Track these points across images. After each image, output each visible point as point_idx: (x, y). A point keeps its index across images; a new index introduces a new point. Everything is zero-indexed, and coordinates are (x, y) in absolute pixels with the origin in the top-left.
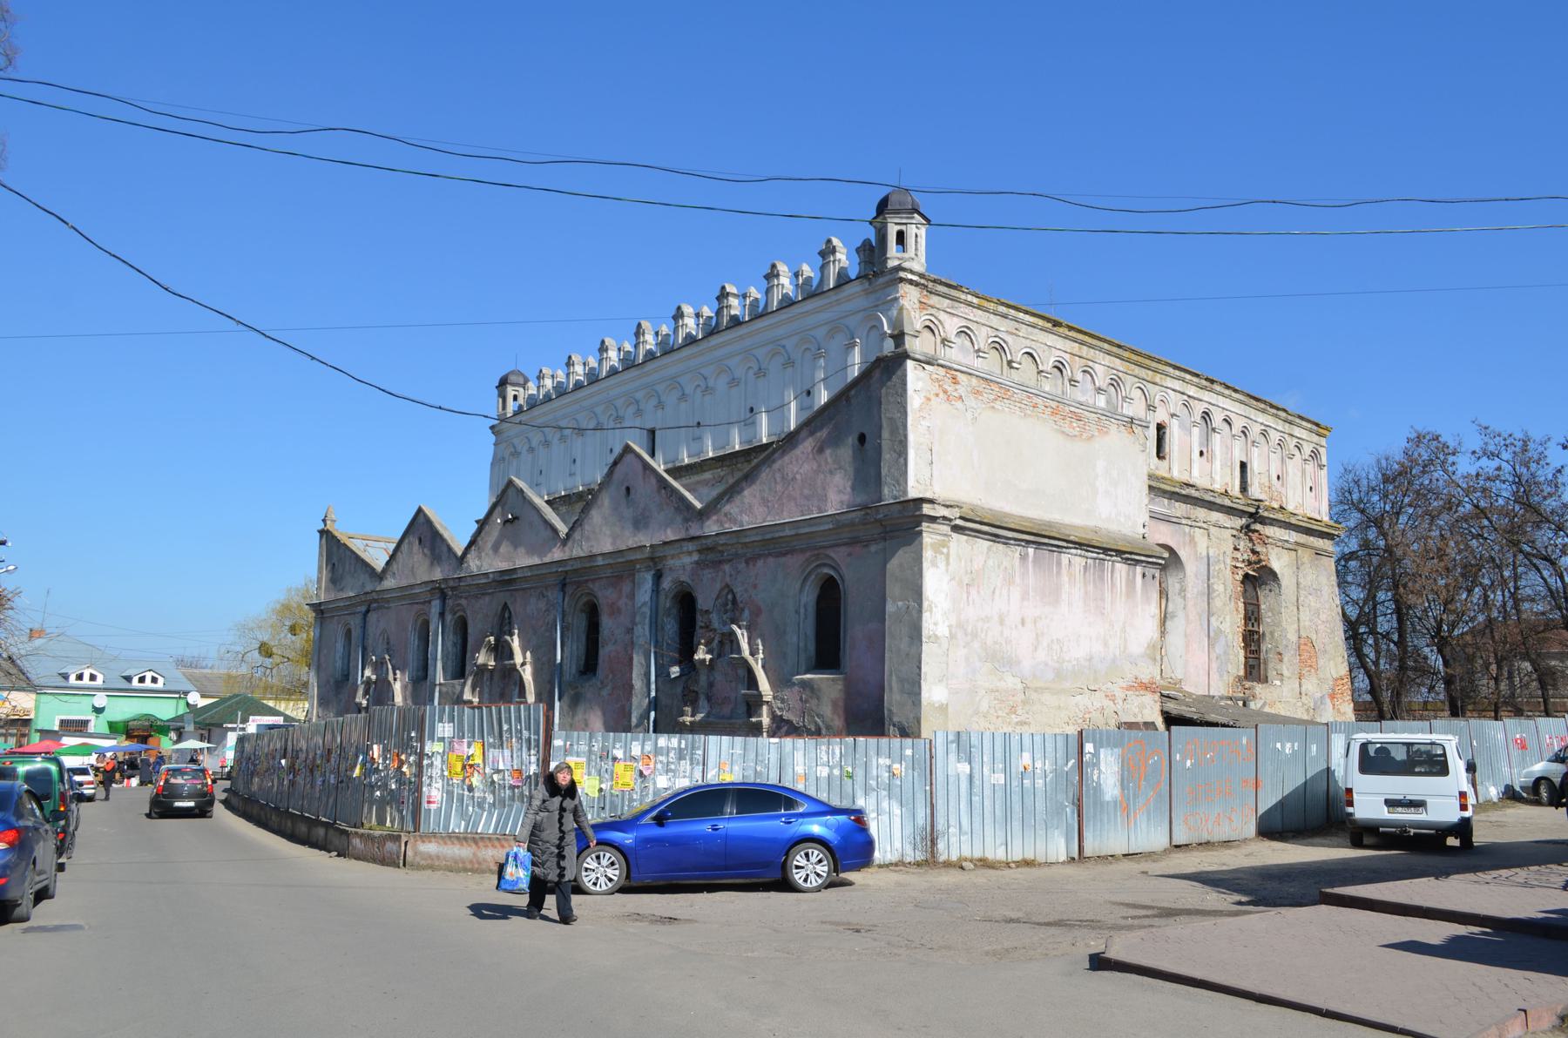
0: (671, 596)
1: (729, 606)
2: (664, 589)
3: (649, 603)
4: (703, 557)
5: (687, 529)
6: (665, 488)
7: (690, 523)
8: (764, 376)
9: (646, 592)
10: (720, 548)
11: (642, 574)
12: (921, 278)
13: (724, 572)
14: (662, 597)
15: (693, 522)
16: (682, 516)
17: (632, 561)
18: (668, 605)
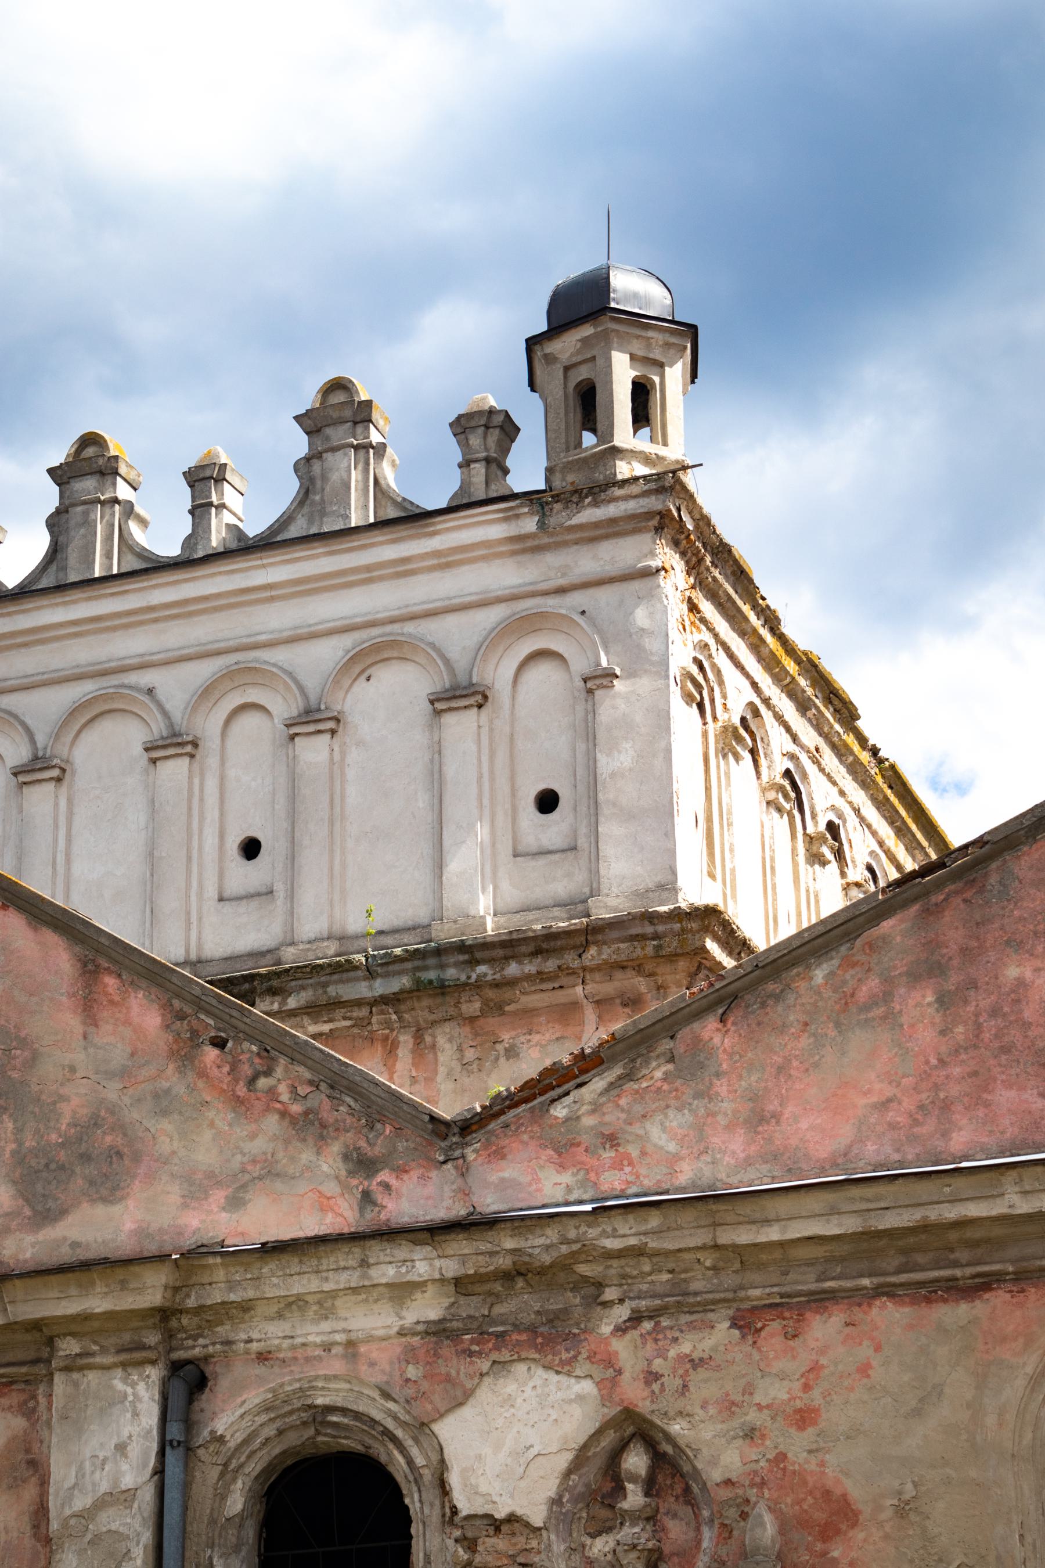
0: (254, 1467)
1: (634, 1498)
2: (221, 1439)
3: (147, 1496)
4: (471, 1307)
5: (367, 1198)
6: (219, 1043)
7: (384, 1176)
8: (59, 780)
9: (121, 1448)
10: (583, 1269)
11: (92, 1376)
12: (697, 527)
13: (609, 1362)
14: (208, 1474)
15: (401, 1171)
16: (336, 1148)
17: (36, 1325)
18: (236, 1503)
